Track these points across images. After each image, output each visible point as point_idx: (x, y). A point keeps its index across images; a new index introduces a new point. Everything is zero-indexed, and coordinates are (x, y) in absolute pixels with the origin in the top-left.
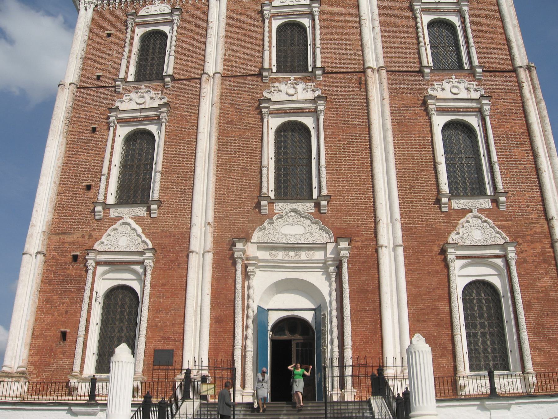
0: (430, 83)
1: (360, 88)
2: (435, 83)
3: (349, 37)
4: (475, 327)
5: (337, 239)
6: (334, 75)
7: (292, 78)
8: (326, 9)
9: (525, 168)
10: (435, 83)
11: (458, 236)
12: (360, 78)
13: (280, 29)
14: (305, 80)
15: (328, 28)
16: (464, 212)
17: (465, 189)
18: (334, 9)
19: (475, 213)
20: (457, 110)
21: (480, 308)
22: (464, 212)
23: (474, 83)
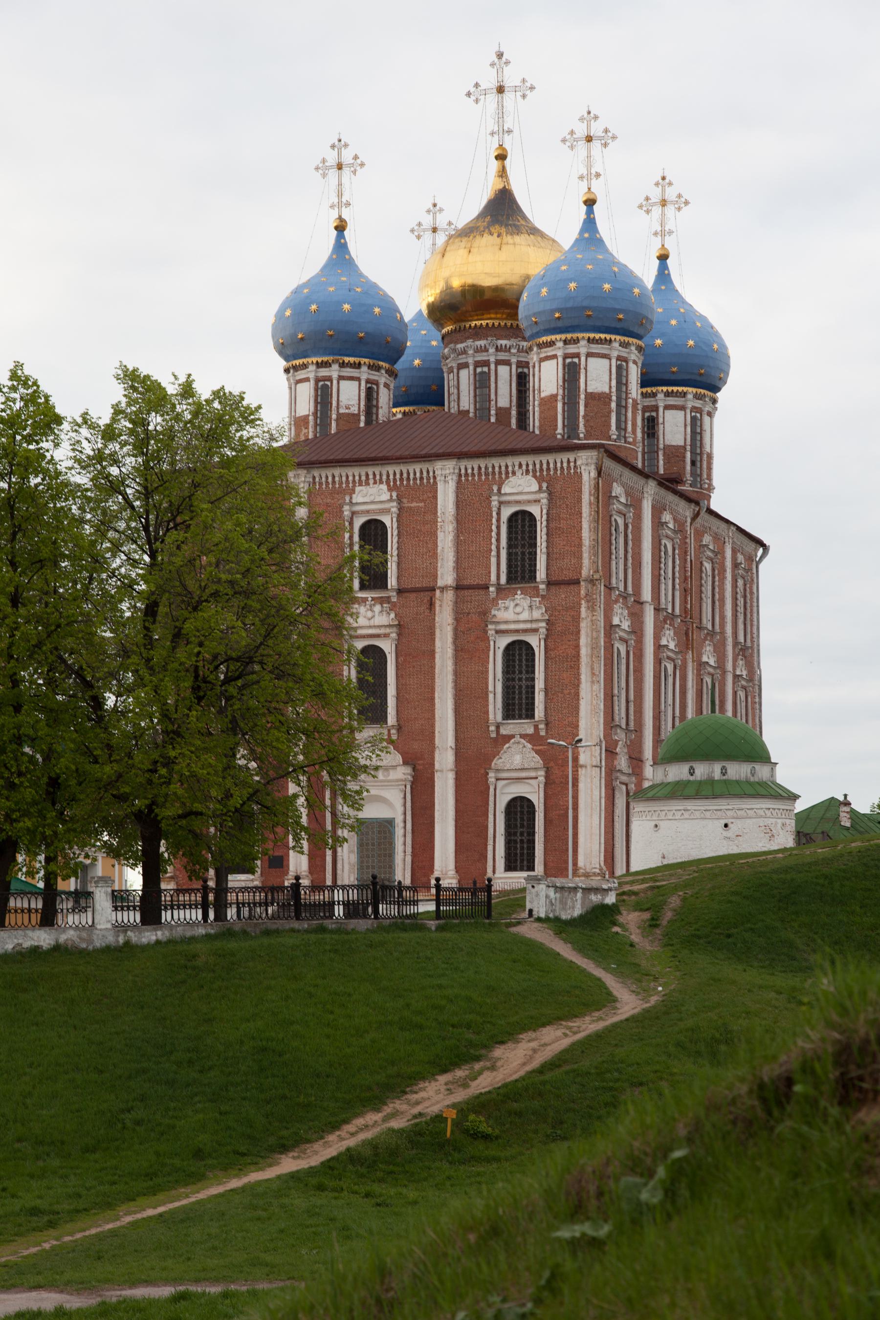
0: (495, 602)
1: (431, 609)
2: (500, 602)
3: (427, 543)
4: (515, 834)
5: (405, 763)
6: (408, 594)
7: (370, 599)
8: (406, 505)
9: (569, 694)
10: (500, 602)
11: (500, 760)
12: (431, 598)
13: (364, 527)
14: (381, 601)
15: (407, 532)
16: (509, 737)
17: (520, 710)
18: (414, 504)
19: (517, 738)
20: (517, 631)
21: (522, 819)
22: (509, 737)
23: (537, 599)
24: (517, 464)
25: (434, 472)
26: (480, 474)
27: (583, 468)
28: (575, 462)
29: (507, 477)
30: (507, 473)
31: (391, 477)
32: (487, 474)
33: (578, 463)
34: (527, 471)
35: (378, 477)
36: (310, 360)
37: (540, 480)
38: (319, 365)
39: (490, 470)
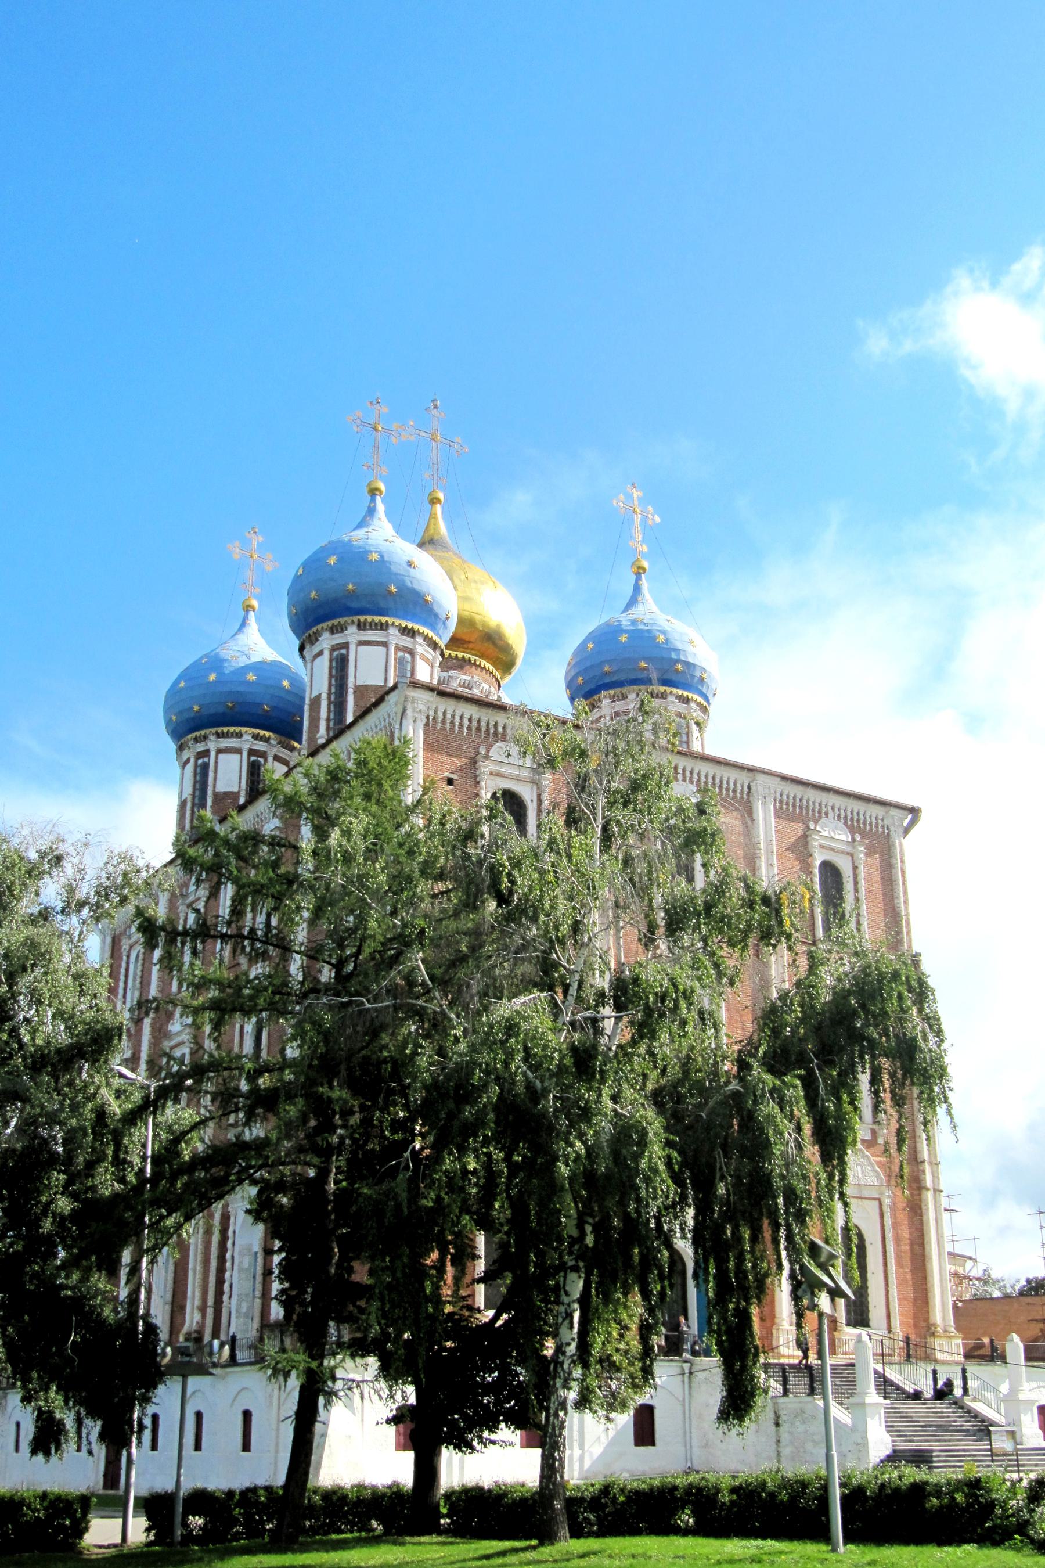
24: (830, 804)
25: (749, 787)
26: (794, 806)
27: (892, 828)
28: (882, 820)
29: (820, 817)
30: (820, 812)
31: (703, 779)
32: (801, 808)
33: (886, 822)
34: (839, 816)
35: (688, 774)
36: (397, 622)
37: (852, 830)
38: (406, 631)
39: (805, 802)
